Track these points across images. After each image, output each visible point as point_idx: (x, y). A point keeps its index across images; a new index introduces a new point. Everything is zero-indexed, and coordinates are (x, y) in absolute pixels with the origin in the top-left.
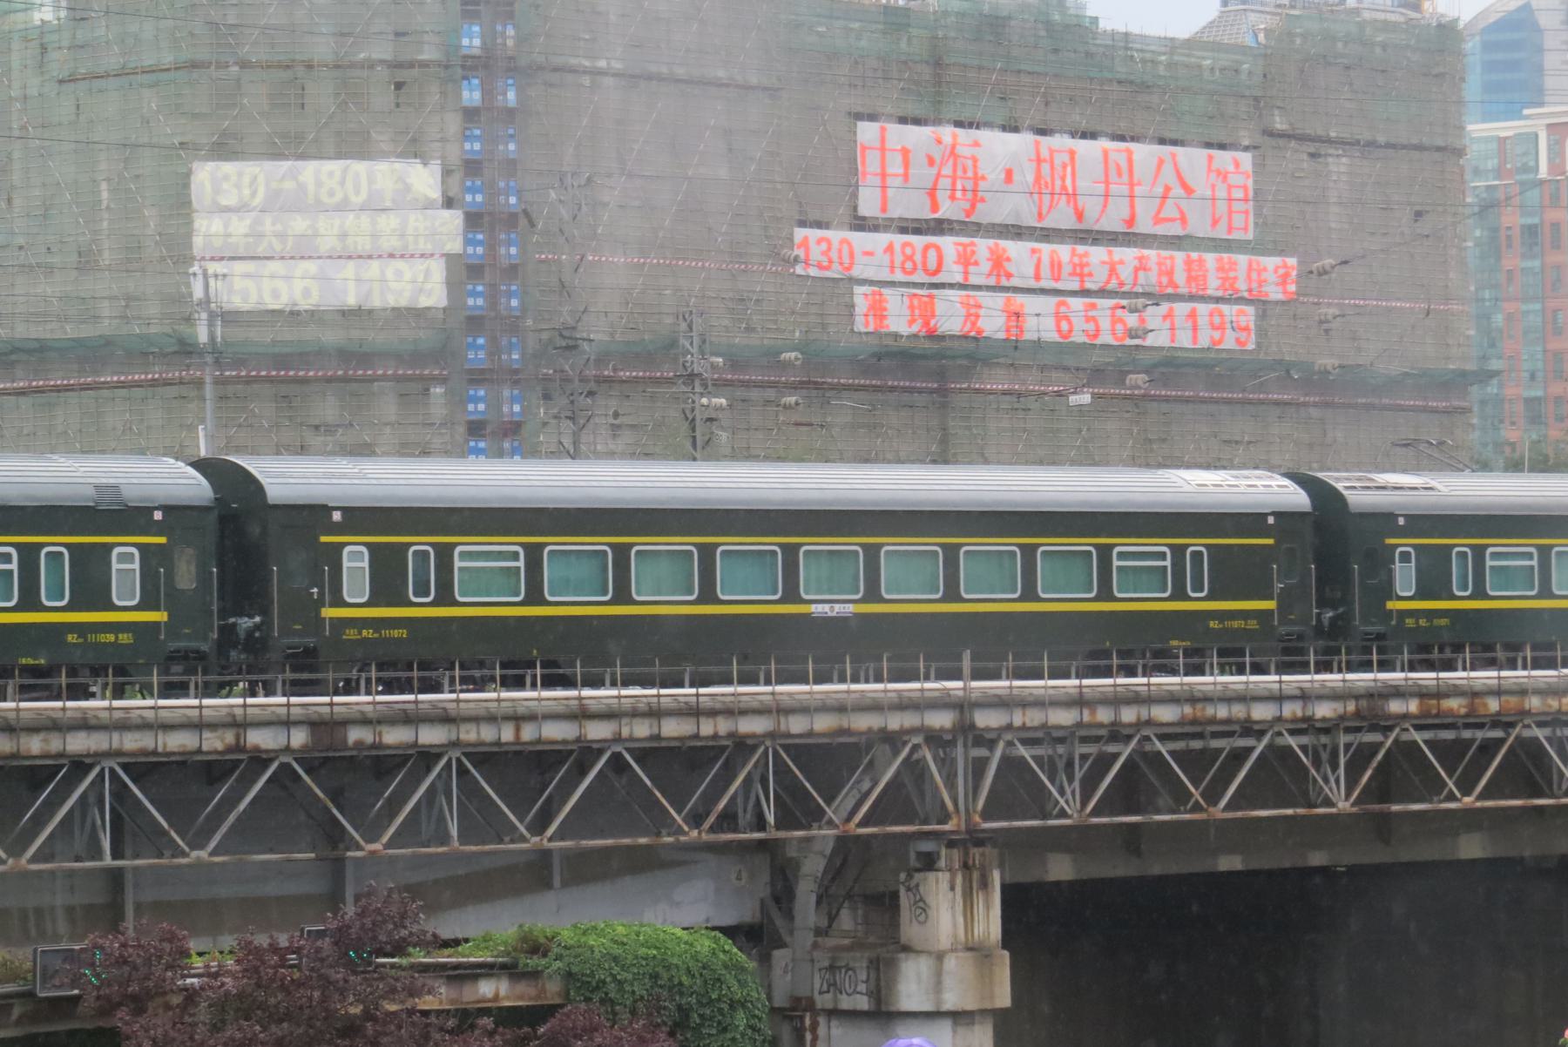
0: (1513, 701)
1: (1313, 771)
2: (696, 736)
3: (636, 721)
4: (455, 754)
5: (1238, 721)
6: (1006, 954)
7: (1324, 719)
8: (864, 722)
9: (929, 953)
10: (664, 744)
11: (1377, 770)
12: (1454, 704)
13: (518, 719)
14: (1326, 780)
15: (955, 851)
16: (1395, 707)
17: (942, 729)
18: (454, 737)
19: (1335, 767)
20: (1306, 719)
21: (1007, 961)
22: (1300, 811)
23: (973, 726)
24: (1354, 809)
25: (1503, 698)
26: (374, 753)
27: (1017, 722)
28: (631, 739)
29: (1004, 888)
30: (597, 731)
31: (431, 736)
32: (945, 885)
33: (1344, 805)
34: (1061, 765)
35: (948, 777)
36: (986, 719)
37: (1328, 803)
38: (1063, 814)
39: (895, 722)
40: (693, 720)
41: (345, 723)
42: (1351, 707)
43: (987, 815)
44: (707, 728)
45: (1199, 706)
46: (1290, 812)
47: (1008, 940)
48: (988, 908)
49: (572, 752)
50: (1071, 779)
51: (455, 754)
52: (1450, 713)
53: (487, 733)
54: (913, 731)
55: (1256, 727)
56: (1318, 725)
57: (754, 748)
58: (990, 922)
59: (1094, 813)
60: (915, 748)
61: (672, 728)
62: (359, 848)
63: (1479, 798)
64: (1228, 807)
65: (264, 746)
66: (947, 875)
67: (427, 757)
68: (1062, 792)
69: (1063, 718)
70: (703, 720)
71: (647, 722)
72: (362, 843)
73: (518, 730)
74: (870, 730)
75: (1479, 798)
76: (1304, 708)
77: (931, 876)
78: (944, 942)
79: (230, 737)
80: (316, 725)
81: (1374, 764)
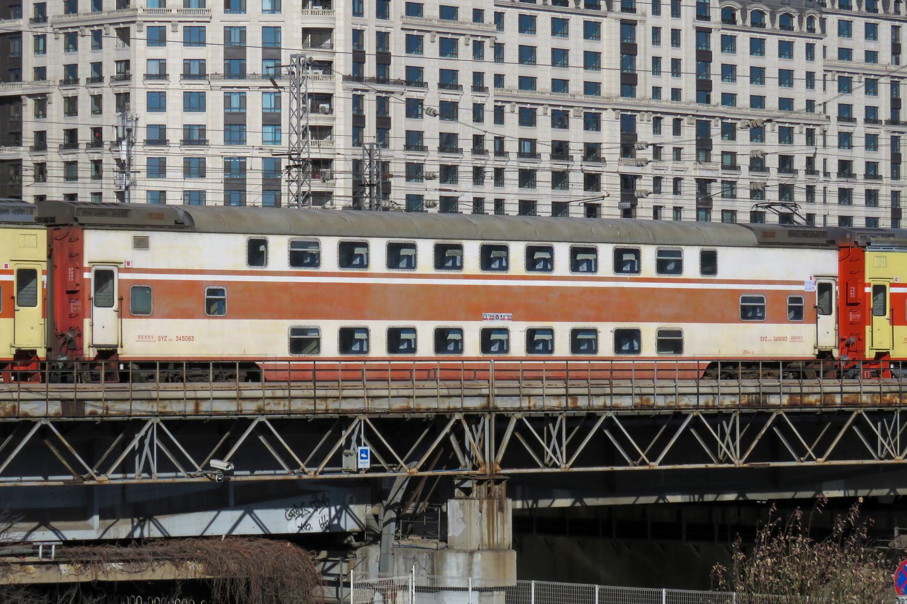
0: (851, 398)
1: (720, 442)
2: (314, 412)
3: (276, 401)
4: (157, 420)
5: (669, 408)
6: (514, 554)
7: (727, 408)
8: (425, 404)
9: (465, 552)
10: (293, 416)
11: (760, 440)
12: (812, 399)
13: (197, 400)
14: (728, 447)
15: (483, 488)
16: (774, 400)
17: (475, 410)
18: (155, 409)
19: (734, 440)
20: (714, 407)
21: (515, 557)
22: (711, 466)
23: (496, 409)
24: (745, 465)
25: (844, 396)
26: (105, 419)
27: (525, 404)
28: (270, 412)
29: (515, 511)
30: (249, 407)
31: (140, 408)
32: (476, 509)
33: (738, 463)
34: (554, 434)
35: (480, 440)
36: (501, 404)
37: (729, 461)
38: (555, 465)
39: (444, 405)
40: (312, 402)
41: (82, 401)
42: (745, 400)
43: (503, 465)
44: (321, 406)
45: (645, 397)
46: (702, 466)
47: (517, 544)
48: (503, 522)
49: (232, 420)
50: (560, 445)
51: (157, 420)
52: (811, 405)
53: (176, 407)
54: (456, 410)
55: (684, 412)
56: (724, 411)
57: (353, 420)
58: (505, 533)
59: (572, 466)
60: (458, 422)
61: (297, 405)
62: (92, 478)
63: (828, 459)
64: (660, 464)
65: (31, 414)
66: (478, 502)
67: (138, 424)
68: (554, 452)
69: (553, 403)
70: (317, 401)
71: (282, 403)
72: (95, 476)
73: (197, 405)
74: (428, 410)
75: (828, 459)
76: (714, 401)
77: (466, 502)
78: (474, 546)
79: (9, 405)
80: (63, 401)
81: (759, 436)
